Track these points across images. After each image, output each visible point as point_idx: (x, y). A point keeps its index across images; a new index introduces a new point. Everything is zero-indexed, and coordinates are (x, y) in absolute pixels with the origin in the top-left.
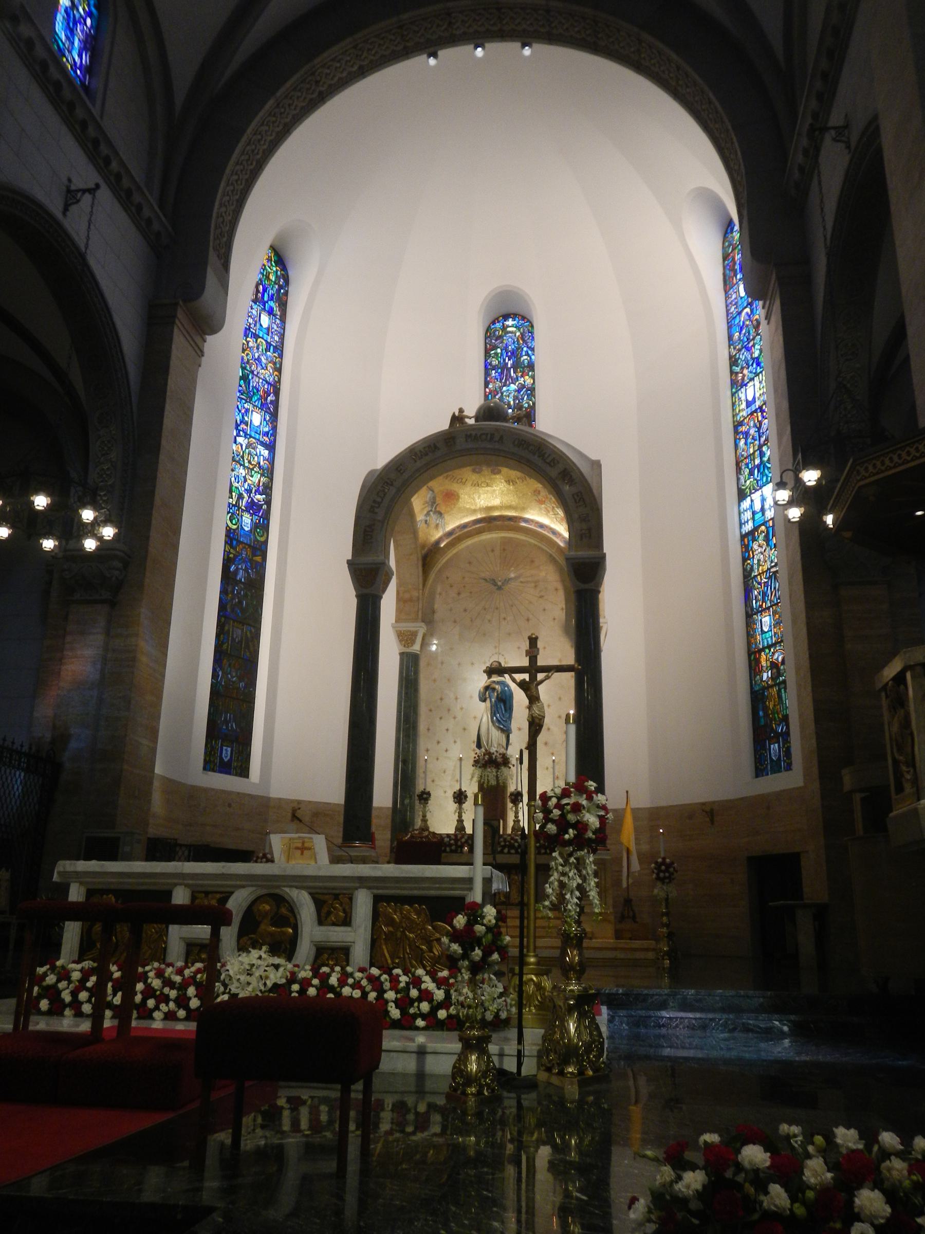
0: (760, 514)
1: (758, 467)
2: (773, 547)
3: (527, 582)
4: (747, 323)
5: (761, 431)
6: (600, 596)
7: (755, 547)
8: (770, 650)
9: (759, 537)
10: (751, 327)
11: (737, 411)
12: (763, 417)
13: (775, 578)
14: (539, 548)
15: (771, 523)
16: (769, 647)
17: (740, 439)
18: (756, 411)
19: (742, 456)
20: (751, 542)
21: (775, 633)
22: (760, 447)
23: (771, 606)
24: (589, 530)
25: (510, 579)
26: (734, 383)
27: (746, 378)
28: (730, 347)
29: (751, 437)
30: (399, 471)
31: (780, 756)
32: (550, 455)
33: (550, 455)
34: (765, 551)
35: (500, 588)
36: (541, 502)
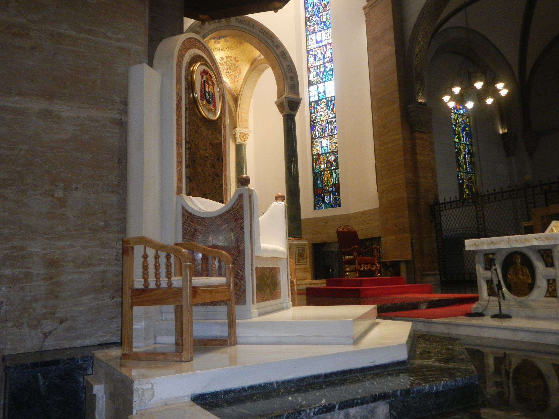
0: (323, 94)
1: (322, 72)
2: (330, 109)
4: (318, 4)
5: (325, 56)
8: (326, 155)
9: (321, 104)
10: (321, 7)
12: (327, 50)
13: (331, 123)
15: (329, 99)
16: (326, 154)
18: (322, 46)
19: (312, 65)
20: (316, 106)
21: (330, 148)
22: (324, 63)
27: (316, 30)
28: (305, 12)
29: (318, 58)
30: (201, 28)
31: (330, 202)
32: (276, 42)
33: (276, 42)
34: (325, 111)
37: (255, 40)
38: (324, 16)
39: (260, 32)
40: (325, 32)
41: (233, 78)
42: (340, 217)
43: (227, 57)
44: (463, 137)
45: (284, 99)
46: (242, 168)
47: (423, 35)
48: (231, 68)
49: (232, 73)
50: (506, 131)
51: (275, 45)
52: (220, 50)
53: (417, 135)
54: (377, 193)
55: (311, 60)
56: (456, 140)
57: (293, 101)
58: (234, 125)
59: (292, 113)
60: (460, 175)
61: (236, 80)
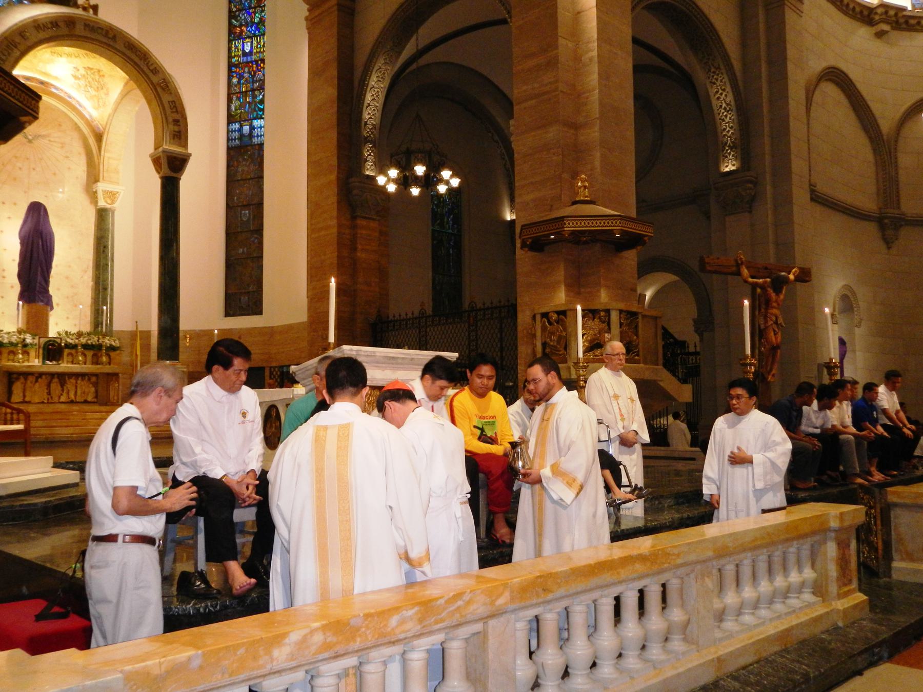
1: (250, 103)
3: (55, 142)
6: (181, 183)
7: (240, 160)
11: (233, 54)
12: (258, 69)
14: (66, 115)
15: (257, 147)
17: (233, 77)
18: (252, 62)
23: (252, 205)
24: (179, 132)
25: (39, 136)
26: (230, 32)
32: (152, 64)
33: (152, 64)
34: (249, 165)
35: (30, 141)
36: (76, 77)
37: (118, 58)
38: (257, 15)
39: (125, 47)
40: (257, 39)
41: (96, 101)
42: (261, 331)
43: (85, 68)
44: (448, 222)
45: (161, 154)
46: (105, 247)
47: (377, 77)
48: (93, 86)
49: (96, 93)
50: (514, 217)
51: (151, 68)
52: (73, 56)
53: (360, 222)
54: (307, 300)
55: (235, 80)
56: (437, 228)
57: (175, 158)
58: (95, 178)
59: (174, 175)
60: (437, 279)
61: (101, 104)
